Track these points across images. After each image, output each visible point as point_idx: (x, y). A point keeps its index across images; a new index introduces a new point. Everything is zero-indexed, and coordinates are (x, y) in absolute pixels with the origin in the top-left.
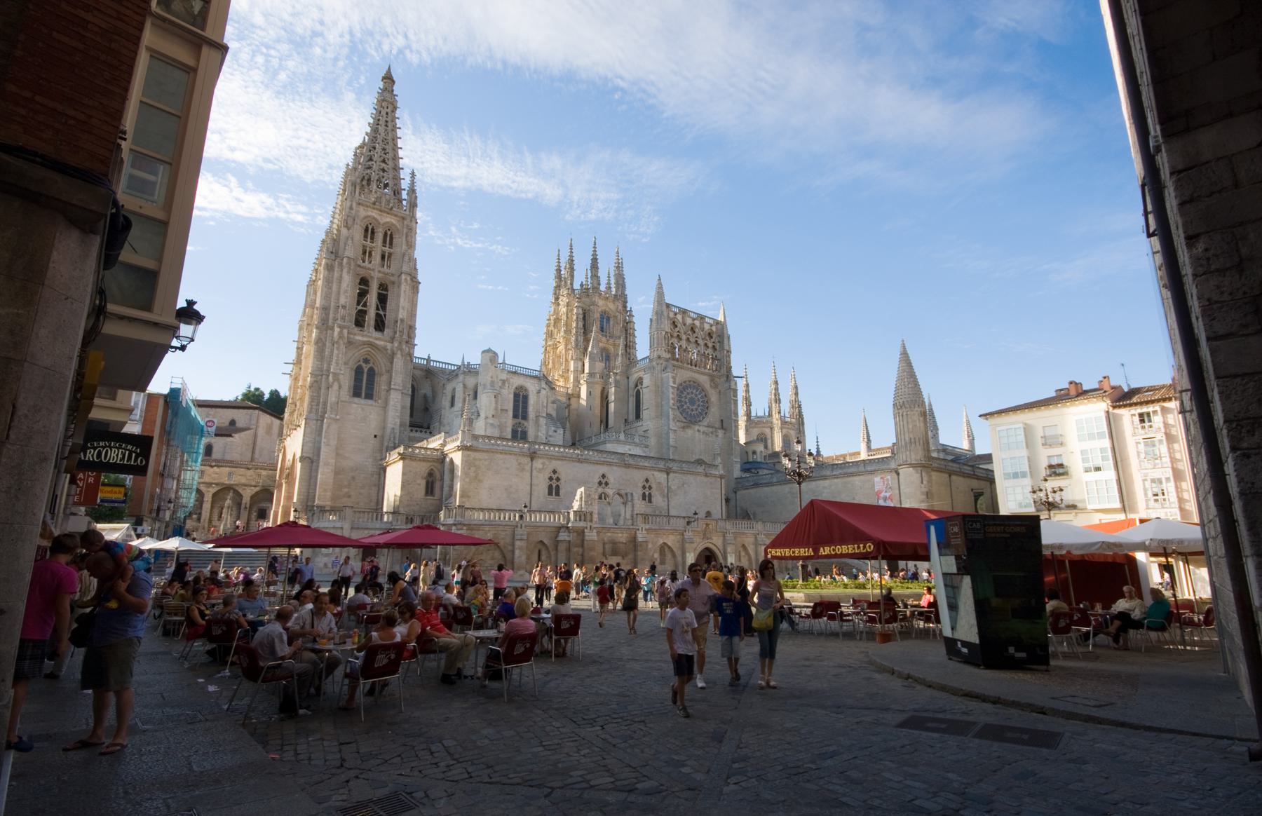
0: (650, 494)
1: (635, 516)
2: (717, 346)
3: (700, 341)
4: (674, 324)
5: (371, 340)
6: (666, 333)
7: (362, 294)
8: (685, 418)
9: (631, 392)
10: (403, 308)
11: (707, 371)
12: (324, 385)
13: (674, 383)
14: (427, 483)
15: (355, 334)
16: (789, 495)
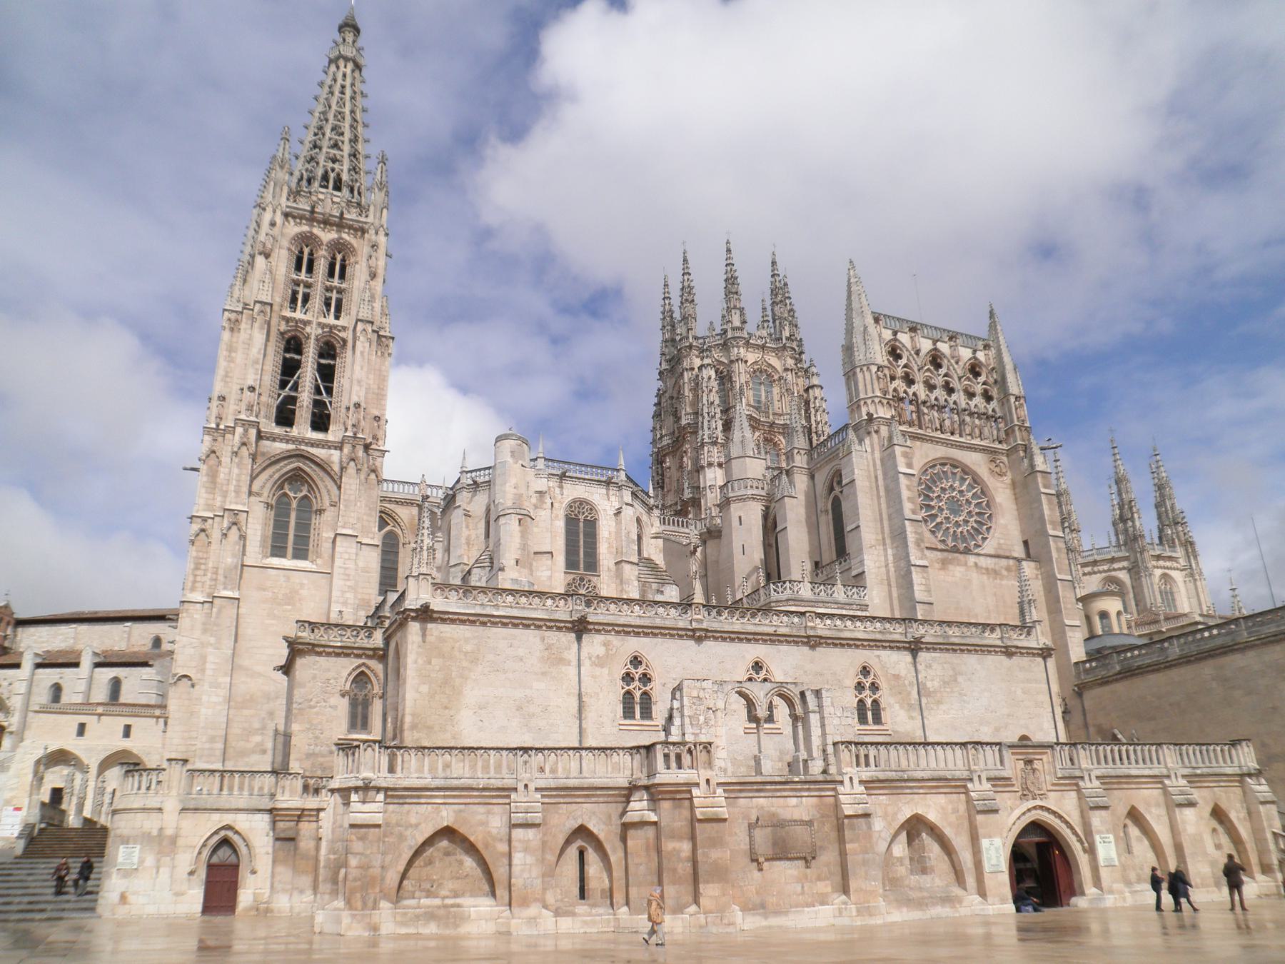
0: (875, 702)
1: (830, 749)
2: (994, 392)
3: (955, 384)
4: (895, 353)
5: (303, 447)
6: (880, 368)
7: (289, 369)
8: (943, 541)
9: (820, 505)
10: (359, 382)
11: (977, 441)
12: (216, 534)
13: (910, 466)
14: (354, 704)
15: (274, 440)
16: (1214, 684)
